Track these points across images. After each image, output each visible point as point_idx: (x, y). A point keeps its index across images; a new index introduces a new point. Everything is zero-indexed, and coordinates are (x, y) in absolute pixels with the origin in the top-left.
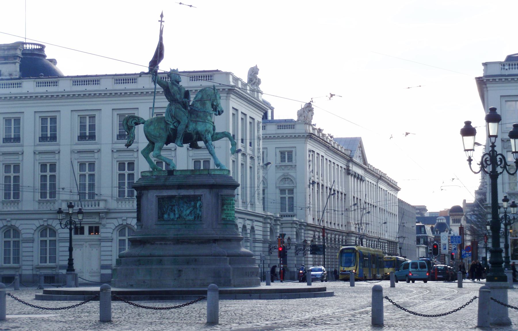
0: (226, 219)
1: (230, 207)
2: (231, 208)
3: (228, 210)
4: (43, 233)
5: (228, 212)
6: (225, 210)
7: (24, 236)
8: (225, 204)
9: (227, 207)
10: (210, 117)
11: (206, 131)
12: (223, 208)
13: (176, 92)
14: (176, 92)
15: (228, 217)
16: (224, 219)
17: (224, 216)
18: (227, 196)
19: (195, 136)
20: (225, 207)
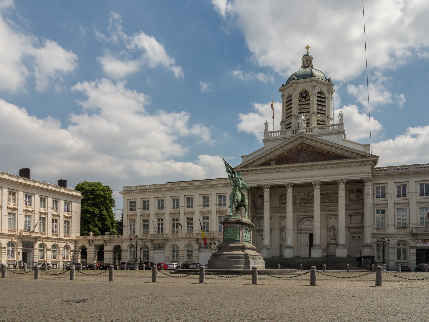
7: (180, 248)
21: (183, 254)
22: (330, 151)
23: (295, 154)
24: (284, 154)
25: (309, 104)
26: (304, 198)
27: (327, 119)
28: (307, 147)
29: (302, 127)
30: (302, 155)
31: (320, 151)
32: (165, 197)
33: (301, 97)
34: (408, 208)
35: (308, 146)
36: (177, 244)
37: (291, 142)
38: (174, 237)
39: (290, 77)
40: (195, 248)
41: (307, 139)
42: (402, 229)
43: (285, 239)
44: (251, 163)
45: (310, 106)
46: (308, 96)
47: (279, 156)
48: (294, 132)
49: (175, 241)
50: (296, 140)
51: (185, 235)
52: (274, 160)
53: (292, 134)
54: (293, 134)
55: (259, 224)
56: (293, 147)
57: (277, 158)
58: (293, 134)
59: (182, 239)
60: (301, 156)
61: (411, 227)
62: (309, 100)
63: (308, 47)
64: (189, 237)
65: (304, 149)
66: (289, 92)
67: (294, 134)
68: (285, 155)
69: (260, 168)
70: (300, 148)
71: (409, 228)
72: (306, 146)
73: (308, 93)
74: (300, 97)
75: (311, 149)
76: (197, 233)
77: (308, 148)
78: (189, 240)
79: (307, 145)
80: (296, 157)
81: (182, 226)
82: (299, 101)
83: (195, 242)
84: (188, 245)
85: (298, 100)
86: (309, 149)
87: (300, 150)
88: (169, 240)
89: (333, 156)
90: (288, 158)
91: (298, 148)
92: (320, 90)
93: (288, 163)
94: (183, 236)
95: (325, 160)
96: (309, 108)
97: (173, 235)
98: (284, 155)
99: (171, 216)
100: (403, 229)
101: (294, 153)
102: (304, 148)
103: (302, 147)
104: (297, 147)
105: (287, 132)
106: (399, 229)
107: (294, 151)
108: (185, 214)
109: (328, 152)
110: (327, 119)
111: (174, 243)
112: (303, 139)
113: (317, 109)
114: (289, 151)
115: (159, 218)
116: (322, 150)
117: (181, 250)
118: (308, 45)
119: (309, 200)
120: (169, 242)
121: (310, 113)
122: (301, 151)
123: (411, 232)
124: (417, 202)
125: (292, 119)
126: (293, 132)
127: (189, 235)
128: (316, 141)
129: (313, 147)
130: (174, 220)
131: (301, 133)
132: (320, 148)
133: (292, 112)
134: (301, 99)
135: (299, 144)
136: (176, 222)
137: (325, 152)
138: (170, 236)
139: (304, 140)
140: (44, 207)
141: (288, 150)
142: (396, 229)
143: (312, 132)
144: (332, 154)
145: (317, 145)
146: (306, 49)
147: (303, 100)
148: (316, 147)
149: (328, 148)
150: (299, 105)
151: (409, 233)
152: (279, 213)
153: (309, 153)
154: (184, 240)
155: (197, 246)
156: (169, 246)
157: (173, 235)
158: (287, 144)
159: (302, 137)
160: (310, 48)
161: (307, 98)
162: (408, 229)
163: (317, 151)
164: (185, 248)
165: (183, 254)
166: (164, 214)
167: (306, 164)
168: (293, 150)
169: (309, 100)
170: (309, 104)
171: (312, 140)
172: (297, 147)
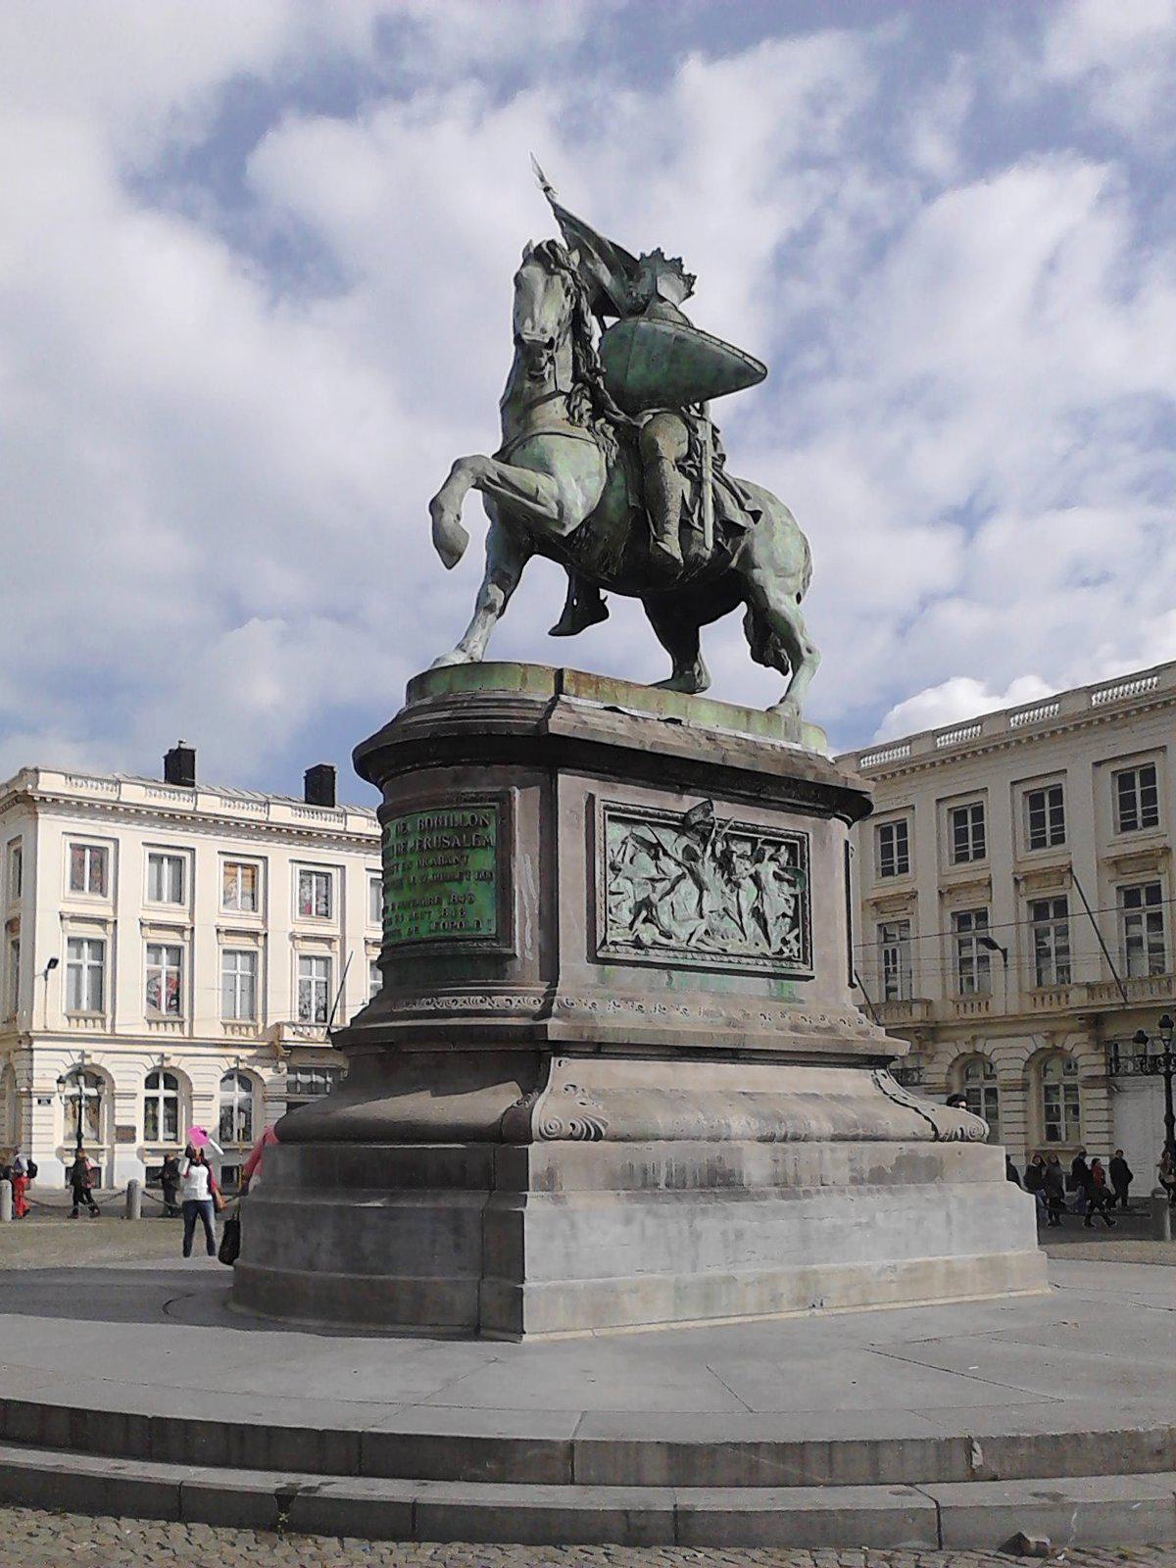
21: (1020, 1106)
32: (913, 807)
36: (986, 1053)
38: (969, 1015)
40: (1088, 1072)
49: (974, 1038)
51: (1028, 1000)
59: (1015, 1023)
64: (1048, 1010)
76: (1089, 986)
78: (1048, 1027)
81: (1004, 952)
83: (1083, 1037)
84: (1041, 1060)
88: (945, 1035)
94: (1014, 1010)
97: (961, 1007)
99: (947, 902)
108: (1022, 883)
111: (968, 1050)
115: (886, 919)
117: (1009, 1088)
120: (941, 1047)
127: (1047, 998)
130: (962, 920)
136: (973, 933)
138: (945, 1012)
140: (178, 898)
154: (1023, 1029)
155: (1094, 1059)
156: (946, 1070)
157: (961, 1007)
164: (1032, 1076)
165: (1020, 1106)
166: (913, 895)
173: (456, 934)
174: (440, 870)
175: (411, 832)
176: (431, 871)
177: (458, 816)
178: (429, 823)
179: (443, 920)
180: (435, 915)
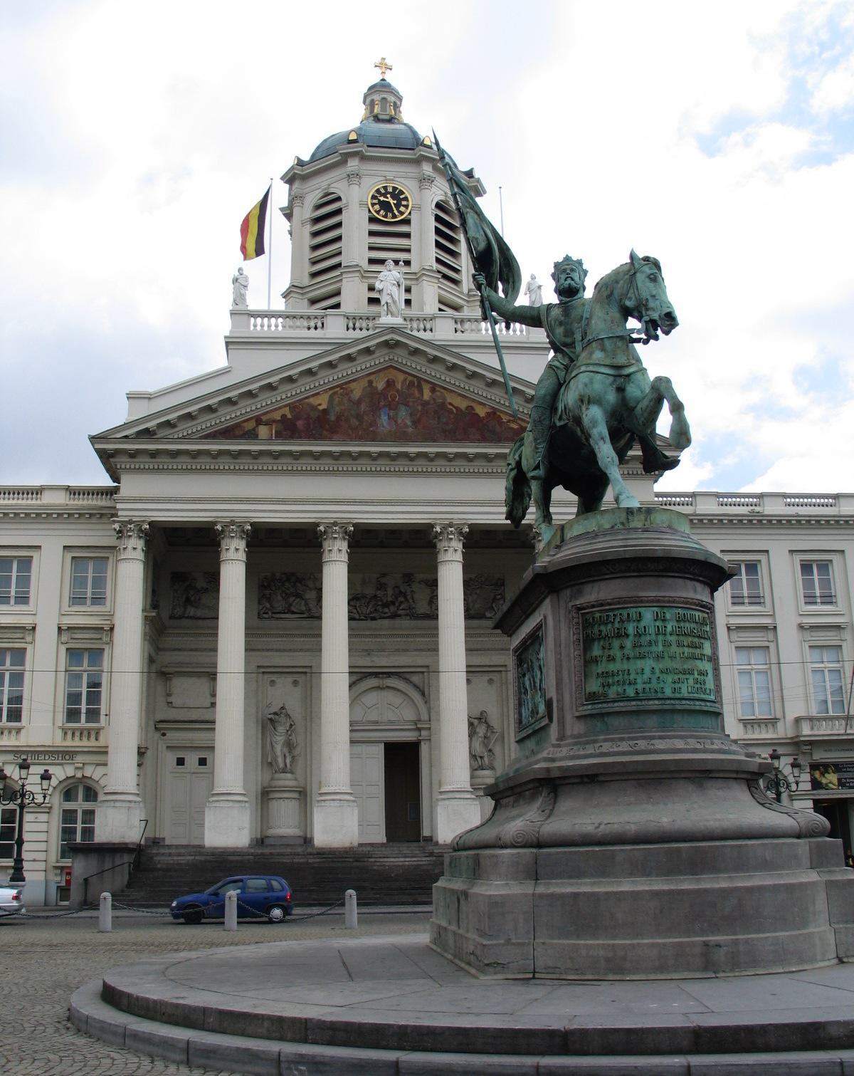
0: (605, 695)
1: (622, 647)
2: (626, 651)
3: (611, 659)
4: (69, 795)
5: (612, 667)
6: (596, 661)
8: (593, 640)
9: (604, 648)
10: (603, 349)
11: (582, 401)
12: (588, 656)
13: (553, 322)
14: (553, 322)
15: (609, 685)
16: (592, 697)
17: (594, 686)
18: (602, 605)
19: (579, 429)
20: (596, 651)
22: (502, 412)
23: (363, 407)
24: (314, 401)
25: (407, 235)
26: (364, 596)
27: (468, 302)
28: (412, 383)
29: (393, 308)
30: (392, 413)
31: (463, 405)
33: (377, 207)
34: (772, 646)
35: (417, 383)
37: (349, 358)
39: (325, 141)
41: (416, 352)
42: (759, 726)
43: (281, 765)
44: (168, 424)
45: (412, 243)
46: (407, 206)
47: (292, 407)
48: (353, 321)
50: (368, 351)
52: (274, 421)
53: (348, 329)
54: (351, 331)
55: (169, 695)
56: (354, 380)
57: (284, 416)
58: (351, 331)
60: (384, 418)
61: (791, 716)
62: (407, 222)
63: (386, 65)
65: (398, 391)
66: (329, 185)
67: (358, 331)
68: (321, 408)
69: (214, 447)
70: (380, 385)
71: (782, 720)
72: (405, 380)
73: (406, 199)
74: (373, 205)
75: (427, 395)
77: (416, 391)
79: (410, 378)
80: (366, 418)
82: (372, 220)
85: (367, 215)
86: (417, 394)
87: (383, 394)
89: (512, 428)
90: (333, 418)
91: (374, 385)
92: (443, 198)
93: (330, 439)
95: (484, 439)
96: (408, 251)
98: (314, 408)
100: (756, 726)
101: (359, 401)
102: (399, 386)
103: (390, 384)
104: (370, 382)
105: (329, 321)
106: (749, 726)
107: (357, 394)
109: (493, 414)
110: (468, 302)
112: (393, 351)
113: (438, 261)
114: (334, 393)
116: (472, 404)
118: (384, 59)
119: (386, 605)
121: (415, 267)
122: (386, 398)
123: (792, 738)
124: (801, 627)
125: (344, 276)
126: (351, 325)
128: (454, 367)
129: (434, 388)
131: (393, 329)
132: (460, 395)
133: (340, 253)
134: (378, 212)
135: (379, 371)
137: (481, 412)
139: (401, 357)
141: (330, 389)
142: (741, 725)
143: (428, 332)
144: (509, 421)
145: (455, 379)
146: (378, 71)
147: (386, 216)
148: (444, 388)
149: (497, 395)
150: (372, 233)
151: (788, 741)
152: (259, 650)
153: (420, 408)
158: (330, 365)
159: (398, 344)
160: (391, 69)
161: (402, 213)
162: (780, 725)
163: (450, 404)
167: (412, 450)
168: (352, 391)
169: (407, 222)
170: (407, 235)
171: (435, 360)
172: (370, 382)
173: (703, 696)
174: (691, 650)
175: (670, 620)
176: (686, 650)
177: (697, 614)
178: (685, 616)
179: (696, 686)
180: (691, 681)
